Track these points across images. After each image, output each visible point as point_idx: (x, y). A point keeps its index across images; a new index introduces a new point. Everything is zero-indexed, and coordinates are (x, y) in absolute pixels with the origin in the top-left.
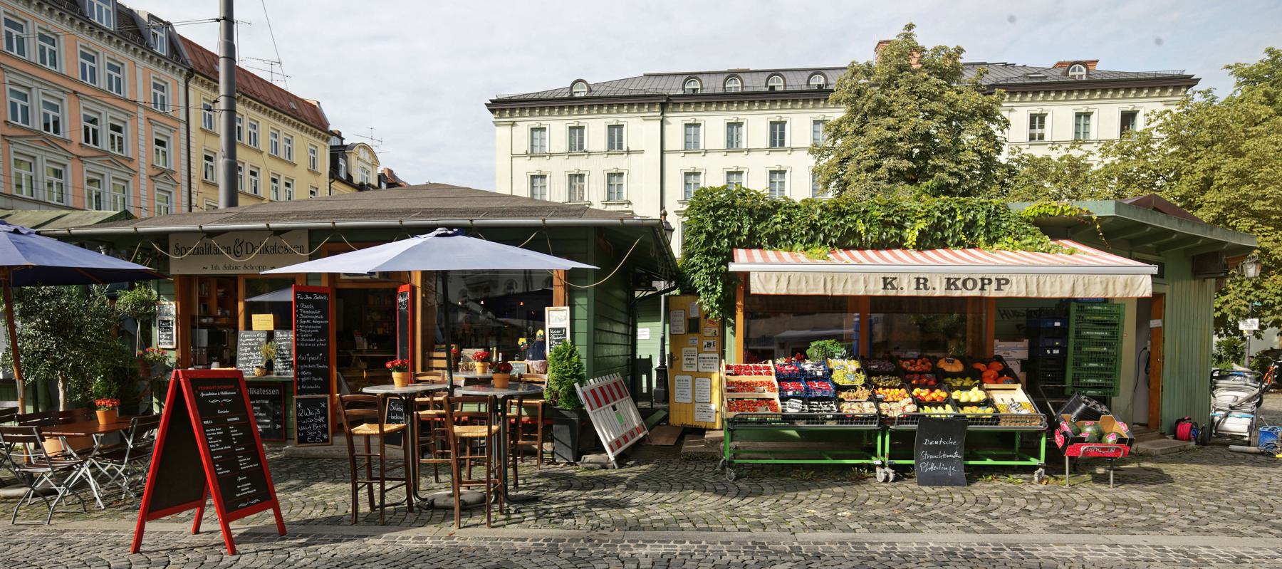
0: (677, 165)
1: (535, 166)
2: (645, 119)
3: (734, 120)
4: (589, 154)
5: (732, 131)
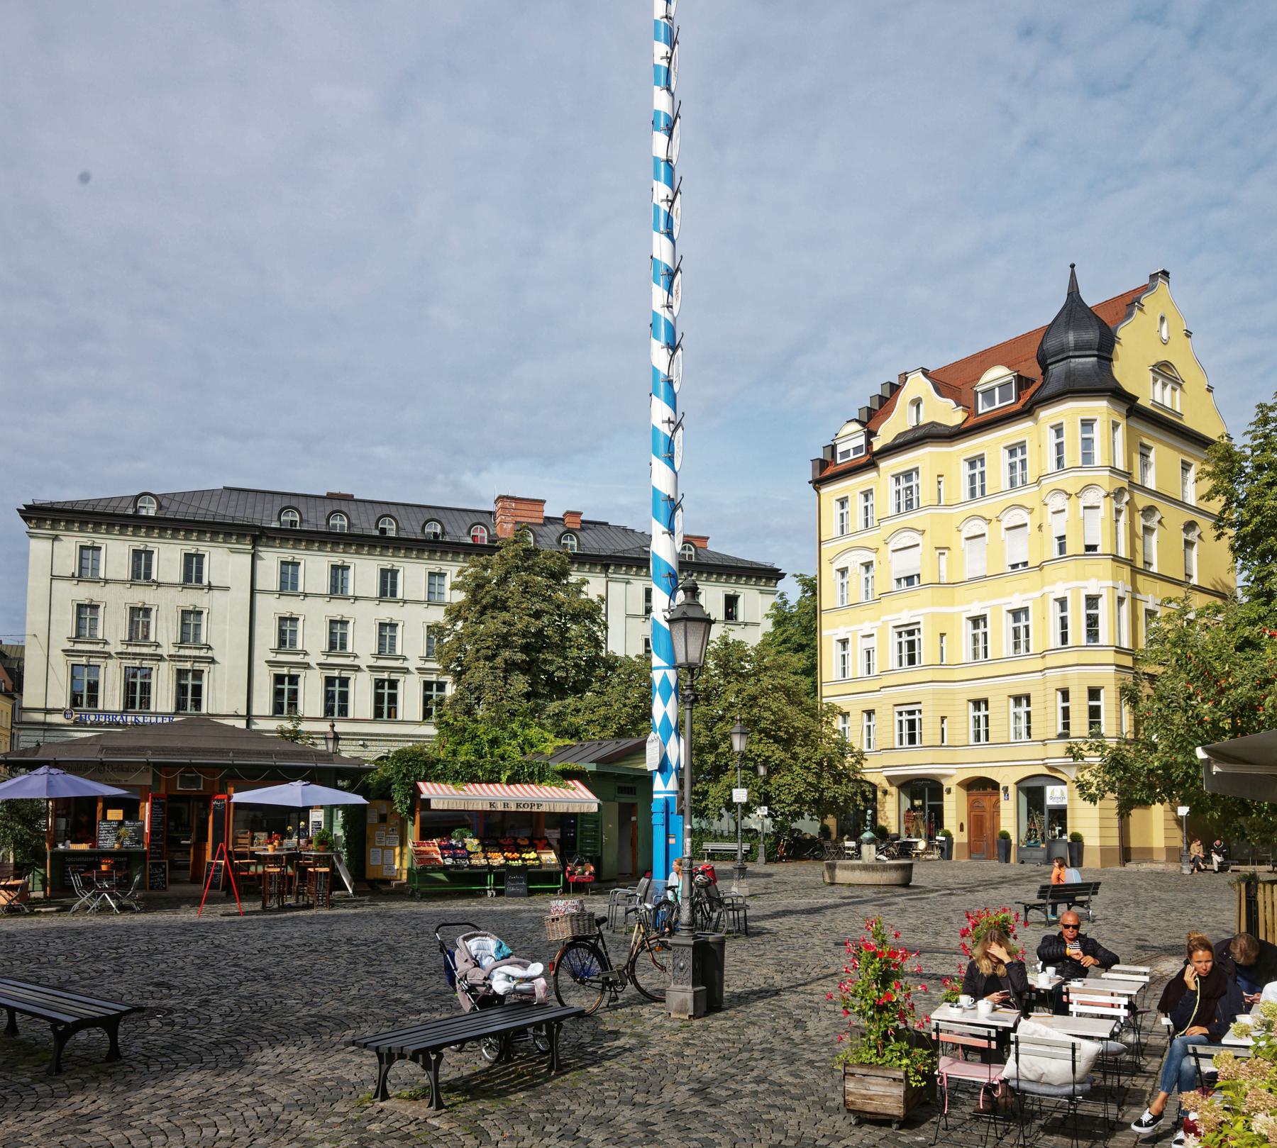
0: (270, 608)
1: (84, 593)
2: (233, 551)
3: (339, 563)
4: (159, 585)
5: (337, 574)
